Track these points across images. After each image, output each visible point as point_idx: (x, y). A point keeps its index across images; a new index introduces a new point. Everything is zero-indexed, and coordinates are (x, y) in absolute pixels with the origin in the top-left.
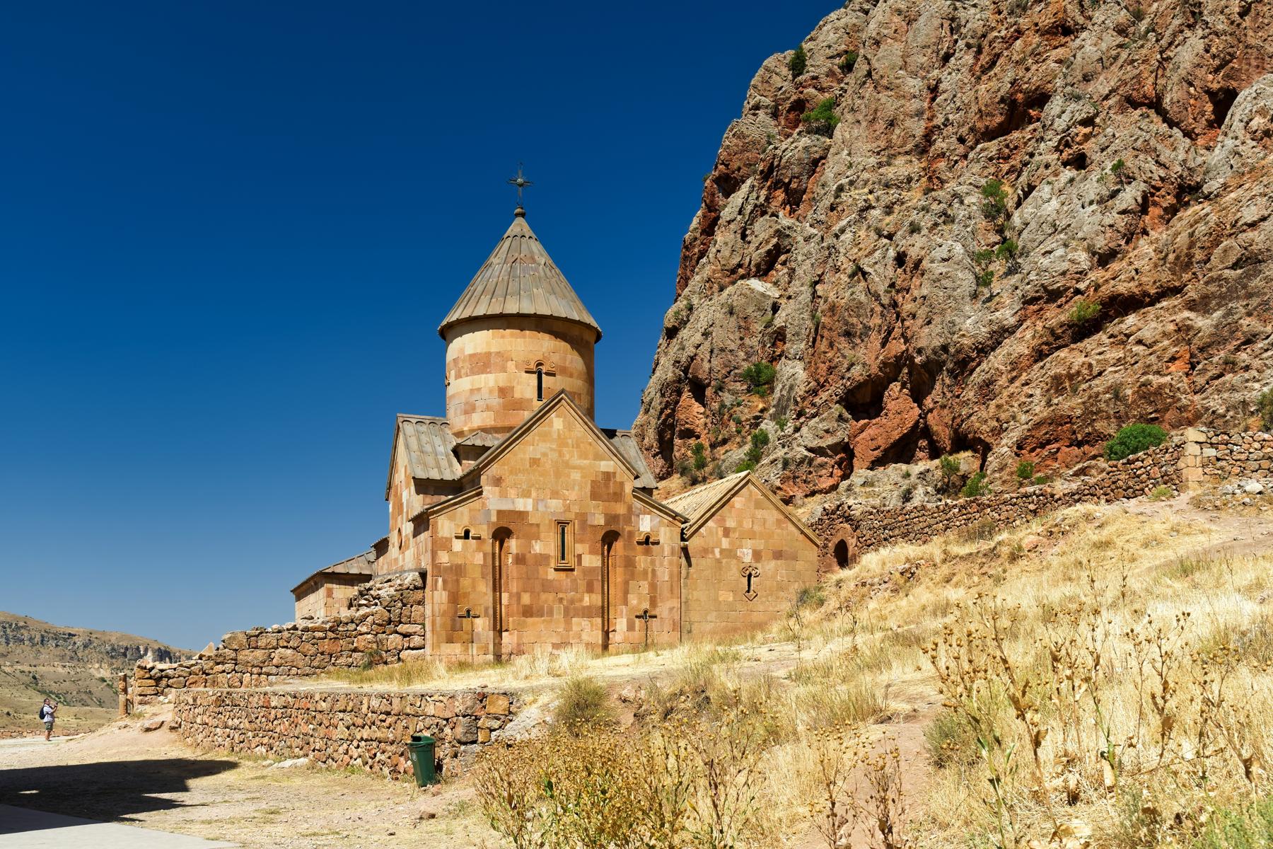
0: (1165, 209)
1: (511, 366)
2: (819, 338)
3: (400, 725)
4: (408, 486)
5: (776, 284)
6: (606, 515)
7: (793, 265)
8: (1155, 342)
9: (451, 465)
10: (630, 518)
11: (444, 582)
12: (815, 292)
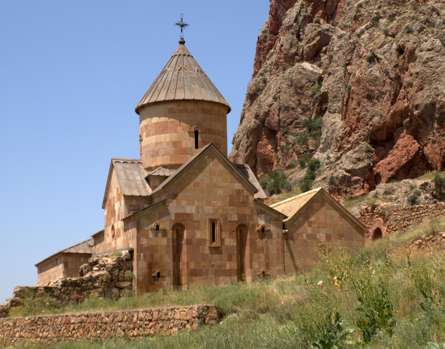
2: (351, 99)
3: (158, 326)
4: (119, 199)
5: (320, 66)
6: (238, 215)
7: (332, 53)
9: (145, 187)
10: (253, 216)
11: (145, 256)
12: (346, 70)
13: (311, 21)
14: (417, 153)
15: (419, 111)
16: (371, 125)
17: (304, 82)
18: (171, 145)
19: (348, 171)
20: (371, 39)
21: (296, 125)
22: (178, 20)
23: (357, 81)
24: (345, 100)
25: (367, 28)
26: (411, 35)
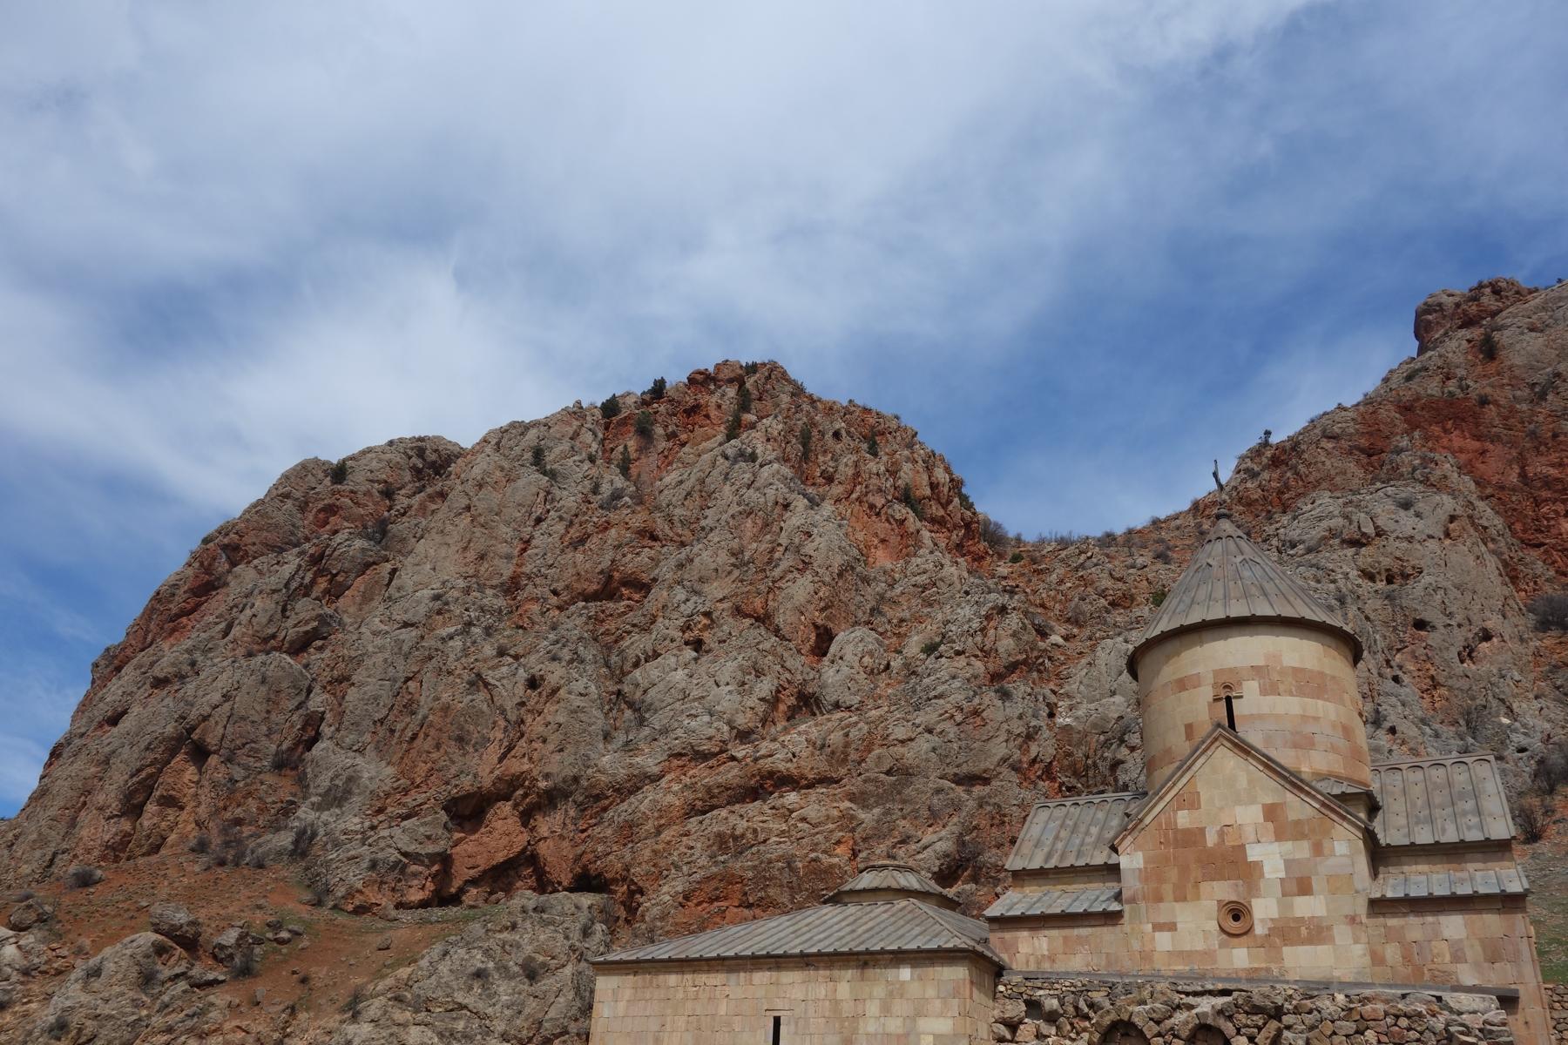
0: (789, 707)
2: (421, 735)
5: (306, 666)
13: (306, 595)
14: (524, 850)
15: (550, 783)
16: (456, 786)
17: (285, 685)
19: (405, 854)
20: (465, 652)
21: (250, 751)
25: (457, 633)
26: (556, 663)
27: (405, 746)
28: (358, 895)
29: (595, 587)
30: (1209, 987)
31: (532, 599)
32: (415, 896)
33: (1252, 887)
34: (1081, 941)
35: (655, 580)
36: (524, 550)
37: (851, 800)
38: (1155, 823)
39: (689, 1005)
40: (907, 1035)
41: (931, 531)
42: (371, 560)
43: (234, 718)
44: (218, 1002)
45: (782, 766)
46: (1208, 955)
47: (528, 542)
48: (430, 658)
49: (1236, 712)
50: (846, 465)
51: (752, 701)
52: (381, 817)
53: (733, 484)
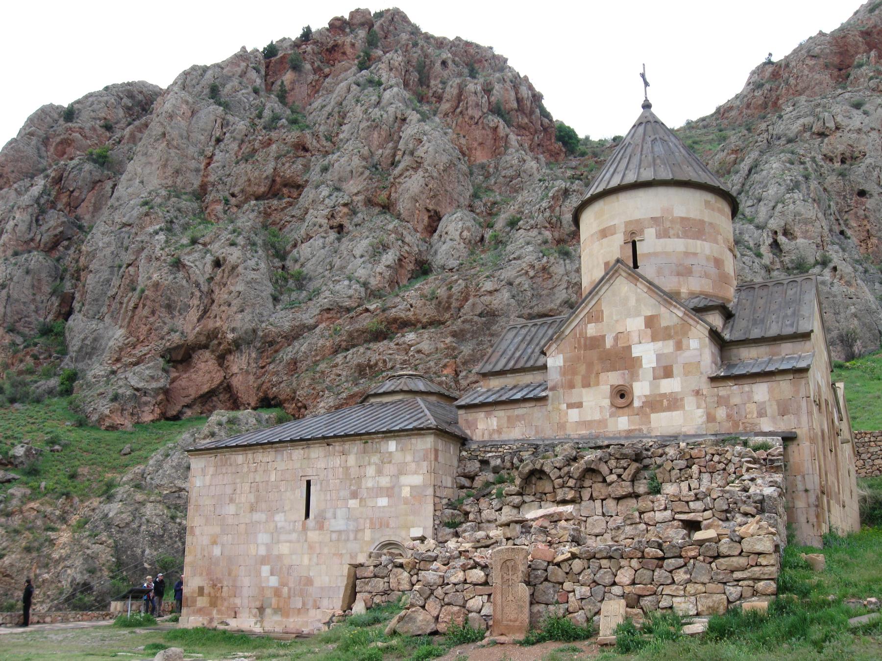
1: (720, 237)
2: (141, 305)
8: (431, 353)
14: (221, 384)
16: (169, 340)
18: (712, 264)
19: (137, 390)
22: (642, 72)
23: (153, 286)
24: (132, 305)
25: (161, 229)
27: (130, 313)
28: (107, 419)
29: (262, 189)
30: (600, 443)
31: (217, 201)
32: (147, 417)
33: (634, 376)
34: (519, 418)
35: (307, 181)
36: (209, 164)
37: (453, 336)
38: (572, 334)
39: (251, 475)
40: (393, 488)
41: (518, 135)
42: (97, 179)
43: (11, 300)
44: (16, 493)
45: (402, 315)
46: (602, 422)
47: (211, 158)
48: (143, 249)
49: (638, 253)
50: (451, 86)
51: (380, 268)
52: (119, 365)
53: (363, 105)
